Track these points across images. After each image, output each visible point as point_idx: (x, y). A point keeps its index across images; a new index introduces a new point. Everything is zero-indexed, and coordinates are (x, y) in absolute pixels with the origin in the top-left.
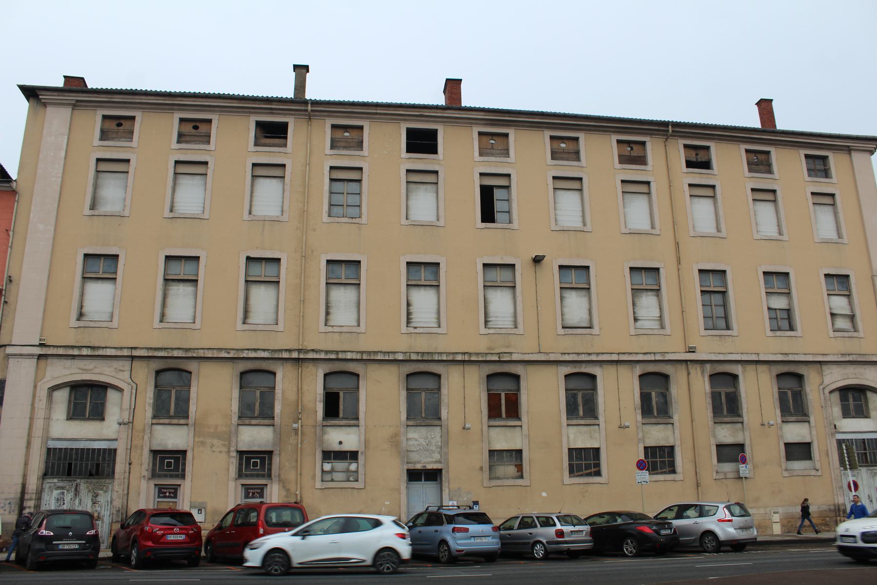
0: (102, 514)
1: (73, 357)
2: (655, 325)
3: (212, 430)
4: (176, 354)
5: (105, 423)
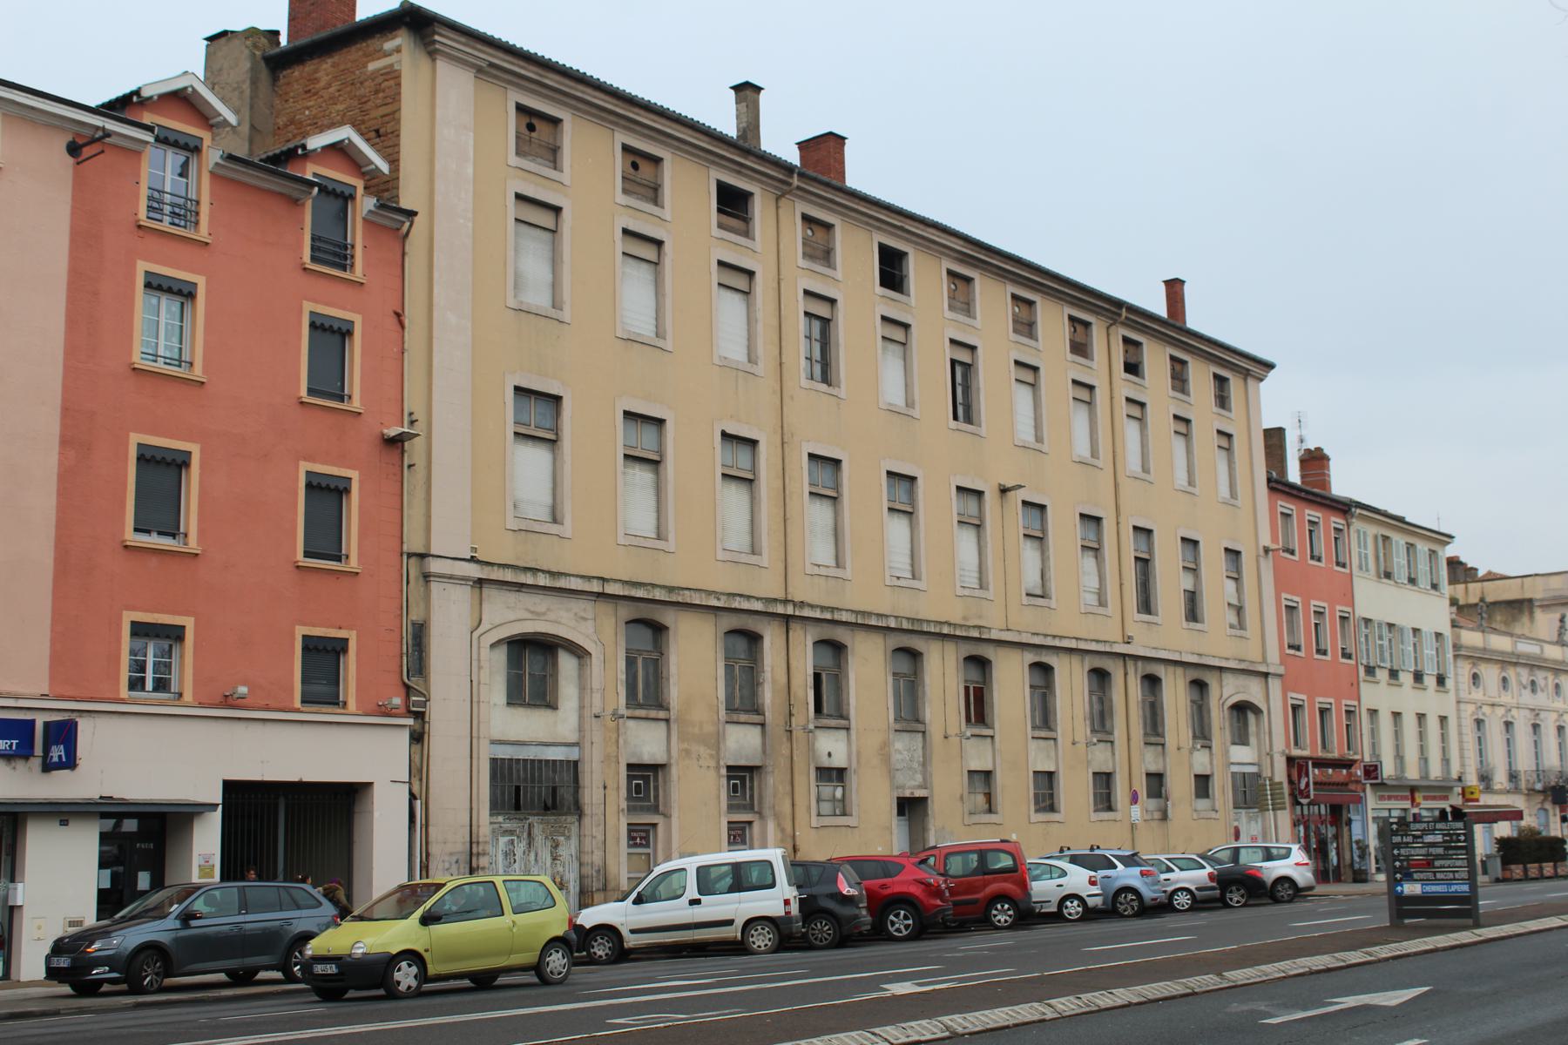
0: (566, 878)
1: (520, 587)
2: (1092, 599)
3: (696, 730)
4: (659, 595)
5: (560, 712)
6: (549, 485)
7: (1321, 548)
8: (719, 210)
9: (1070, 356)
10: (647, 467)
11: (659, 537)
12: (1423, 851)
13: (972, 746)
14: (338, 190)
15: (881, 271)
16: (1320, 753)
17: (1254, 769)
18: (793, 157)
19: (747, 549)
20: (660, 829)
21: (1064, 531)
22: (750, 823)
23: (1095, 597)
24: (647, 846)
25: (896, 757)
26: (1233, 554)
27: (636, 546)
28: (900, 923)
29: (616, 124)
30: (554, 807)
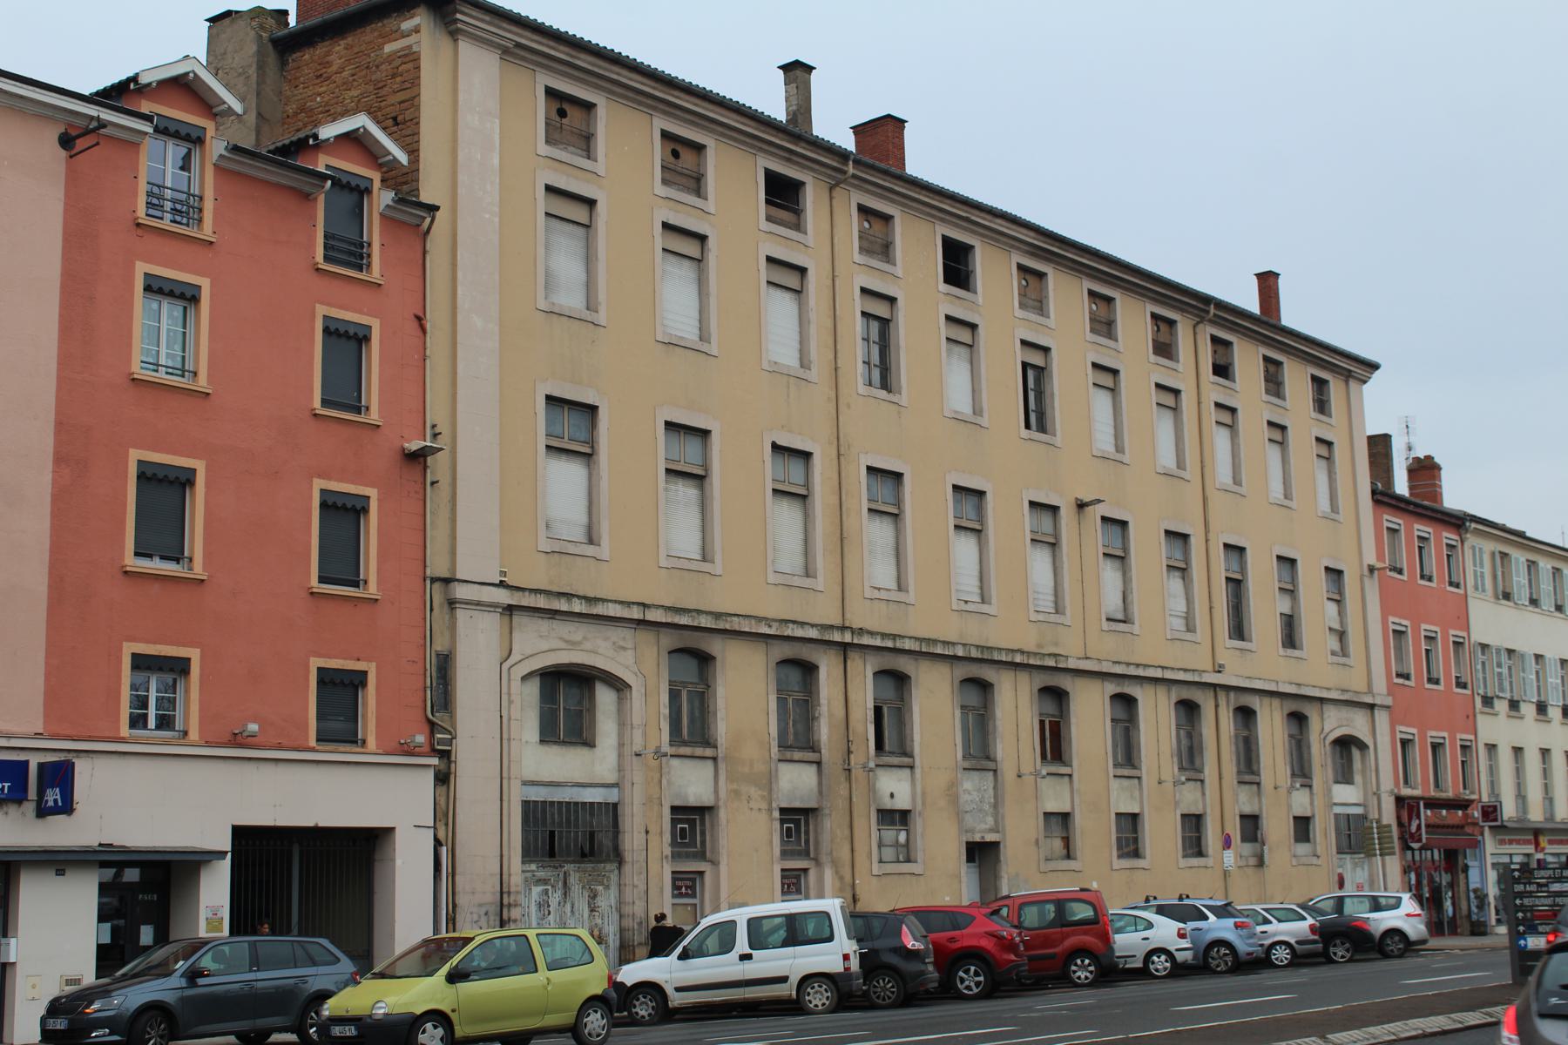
0: (605, 931)
1: (553, 614)
2: (1179, 624)
3: (746, 770)
4: (705, 622)
5: (597, 750)
6: (583, 503)
7: (1432, 566)
8: (768, 202)
9: (1153, 358)
10: (691, 482)
11: (704, 559)
12: (1549, 901)
13: (1047, 786)
14: (353, 184)
15: (945, 265)
16: (1433, 793)
17: (1359, 811)
18: (848, 143)
19: (800, 570)
20: (708, 878)
21: (1148, 549)
22: (805, 870)
23: (1183, 622)
24: (694, 896)
25: (964, 798)
26: (1335, 574)
27: (679, 568)
28: (970, 979)
29: (654, 108)
30: (592, 853)
